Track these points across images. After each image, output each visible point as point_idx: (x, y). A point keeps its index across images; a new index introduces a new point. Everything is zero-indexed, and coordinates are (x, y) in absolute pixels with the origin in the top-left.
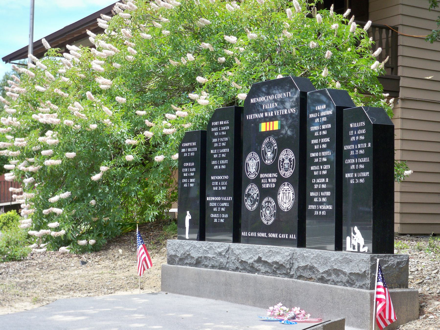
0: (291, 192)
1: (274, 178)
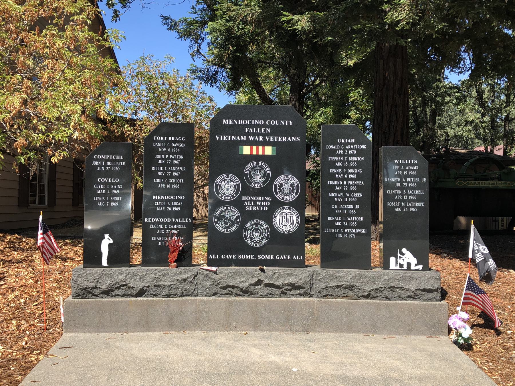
0: (294, 215)
1: (266, 201)
